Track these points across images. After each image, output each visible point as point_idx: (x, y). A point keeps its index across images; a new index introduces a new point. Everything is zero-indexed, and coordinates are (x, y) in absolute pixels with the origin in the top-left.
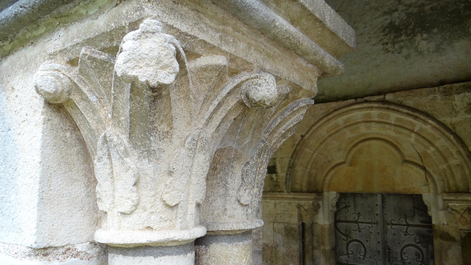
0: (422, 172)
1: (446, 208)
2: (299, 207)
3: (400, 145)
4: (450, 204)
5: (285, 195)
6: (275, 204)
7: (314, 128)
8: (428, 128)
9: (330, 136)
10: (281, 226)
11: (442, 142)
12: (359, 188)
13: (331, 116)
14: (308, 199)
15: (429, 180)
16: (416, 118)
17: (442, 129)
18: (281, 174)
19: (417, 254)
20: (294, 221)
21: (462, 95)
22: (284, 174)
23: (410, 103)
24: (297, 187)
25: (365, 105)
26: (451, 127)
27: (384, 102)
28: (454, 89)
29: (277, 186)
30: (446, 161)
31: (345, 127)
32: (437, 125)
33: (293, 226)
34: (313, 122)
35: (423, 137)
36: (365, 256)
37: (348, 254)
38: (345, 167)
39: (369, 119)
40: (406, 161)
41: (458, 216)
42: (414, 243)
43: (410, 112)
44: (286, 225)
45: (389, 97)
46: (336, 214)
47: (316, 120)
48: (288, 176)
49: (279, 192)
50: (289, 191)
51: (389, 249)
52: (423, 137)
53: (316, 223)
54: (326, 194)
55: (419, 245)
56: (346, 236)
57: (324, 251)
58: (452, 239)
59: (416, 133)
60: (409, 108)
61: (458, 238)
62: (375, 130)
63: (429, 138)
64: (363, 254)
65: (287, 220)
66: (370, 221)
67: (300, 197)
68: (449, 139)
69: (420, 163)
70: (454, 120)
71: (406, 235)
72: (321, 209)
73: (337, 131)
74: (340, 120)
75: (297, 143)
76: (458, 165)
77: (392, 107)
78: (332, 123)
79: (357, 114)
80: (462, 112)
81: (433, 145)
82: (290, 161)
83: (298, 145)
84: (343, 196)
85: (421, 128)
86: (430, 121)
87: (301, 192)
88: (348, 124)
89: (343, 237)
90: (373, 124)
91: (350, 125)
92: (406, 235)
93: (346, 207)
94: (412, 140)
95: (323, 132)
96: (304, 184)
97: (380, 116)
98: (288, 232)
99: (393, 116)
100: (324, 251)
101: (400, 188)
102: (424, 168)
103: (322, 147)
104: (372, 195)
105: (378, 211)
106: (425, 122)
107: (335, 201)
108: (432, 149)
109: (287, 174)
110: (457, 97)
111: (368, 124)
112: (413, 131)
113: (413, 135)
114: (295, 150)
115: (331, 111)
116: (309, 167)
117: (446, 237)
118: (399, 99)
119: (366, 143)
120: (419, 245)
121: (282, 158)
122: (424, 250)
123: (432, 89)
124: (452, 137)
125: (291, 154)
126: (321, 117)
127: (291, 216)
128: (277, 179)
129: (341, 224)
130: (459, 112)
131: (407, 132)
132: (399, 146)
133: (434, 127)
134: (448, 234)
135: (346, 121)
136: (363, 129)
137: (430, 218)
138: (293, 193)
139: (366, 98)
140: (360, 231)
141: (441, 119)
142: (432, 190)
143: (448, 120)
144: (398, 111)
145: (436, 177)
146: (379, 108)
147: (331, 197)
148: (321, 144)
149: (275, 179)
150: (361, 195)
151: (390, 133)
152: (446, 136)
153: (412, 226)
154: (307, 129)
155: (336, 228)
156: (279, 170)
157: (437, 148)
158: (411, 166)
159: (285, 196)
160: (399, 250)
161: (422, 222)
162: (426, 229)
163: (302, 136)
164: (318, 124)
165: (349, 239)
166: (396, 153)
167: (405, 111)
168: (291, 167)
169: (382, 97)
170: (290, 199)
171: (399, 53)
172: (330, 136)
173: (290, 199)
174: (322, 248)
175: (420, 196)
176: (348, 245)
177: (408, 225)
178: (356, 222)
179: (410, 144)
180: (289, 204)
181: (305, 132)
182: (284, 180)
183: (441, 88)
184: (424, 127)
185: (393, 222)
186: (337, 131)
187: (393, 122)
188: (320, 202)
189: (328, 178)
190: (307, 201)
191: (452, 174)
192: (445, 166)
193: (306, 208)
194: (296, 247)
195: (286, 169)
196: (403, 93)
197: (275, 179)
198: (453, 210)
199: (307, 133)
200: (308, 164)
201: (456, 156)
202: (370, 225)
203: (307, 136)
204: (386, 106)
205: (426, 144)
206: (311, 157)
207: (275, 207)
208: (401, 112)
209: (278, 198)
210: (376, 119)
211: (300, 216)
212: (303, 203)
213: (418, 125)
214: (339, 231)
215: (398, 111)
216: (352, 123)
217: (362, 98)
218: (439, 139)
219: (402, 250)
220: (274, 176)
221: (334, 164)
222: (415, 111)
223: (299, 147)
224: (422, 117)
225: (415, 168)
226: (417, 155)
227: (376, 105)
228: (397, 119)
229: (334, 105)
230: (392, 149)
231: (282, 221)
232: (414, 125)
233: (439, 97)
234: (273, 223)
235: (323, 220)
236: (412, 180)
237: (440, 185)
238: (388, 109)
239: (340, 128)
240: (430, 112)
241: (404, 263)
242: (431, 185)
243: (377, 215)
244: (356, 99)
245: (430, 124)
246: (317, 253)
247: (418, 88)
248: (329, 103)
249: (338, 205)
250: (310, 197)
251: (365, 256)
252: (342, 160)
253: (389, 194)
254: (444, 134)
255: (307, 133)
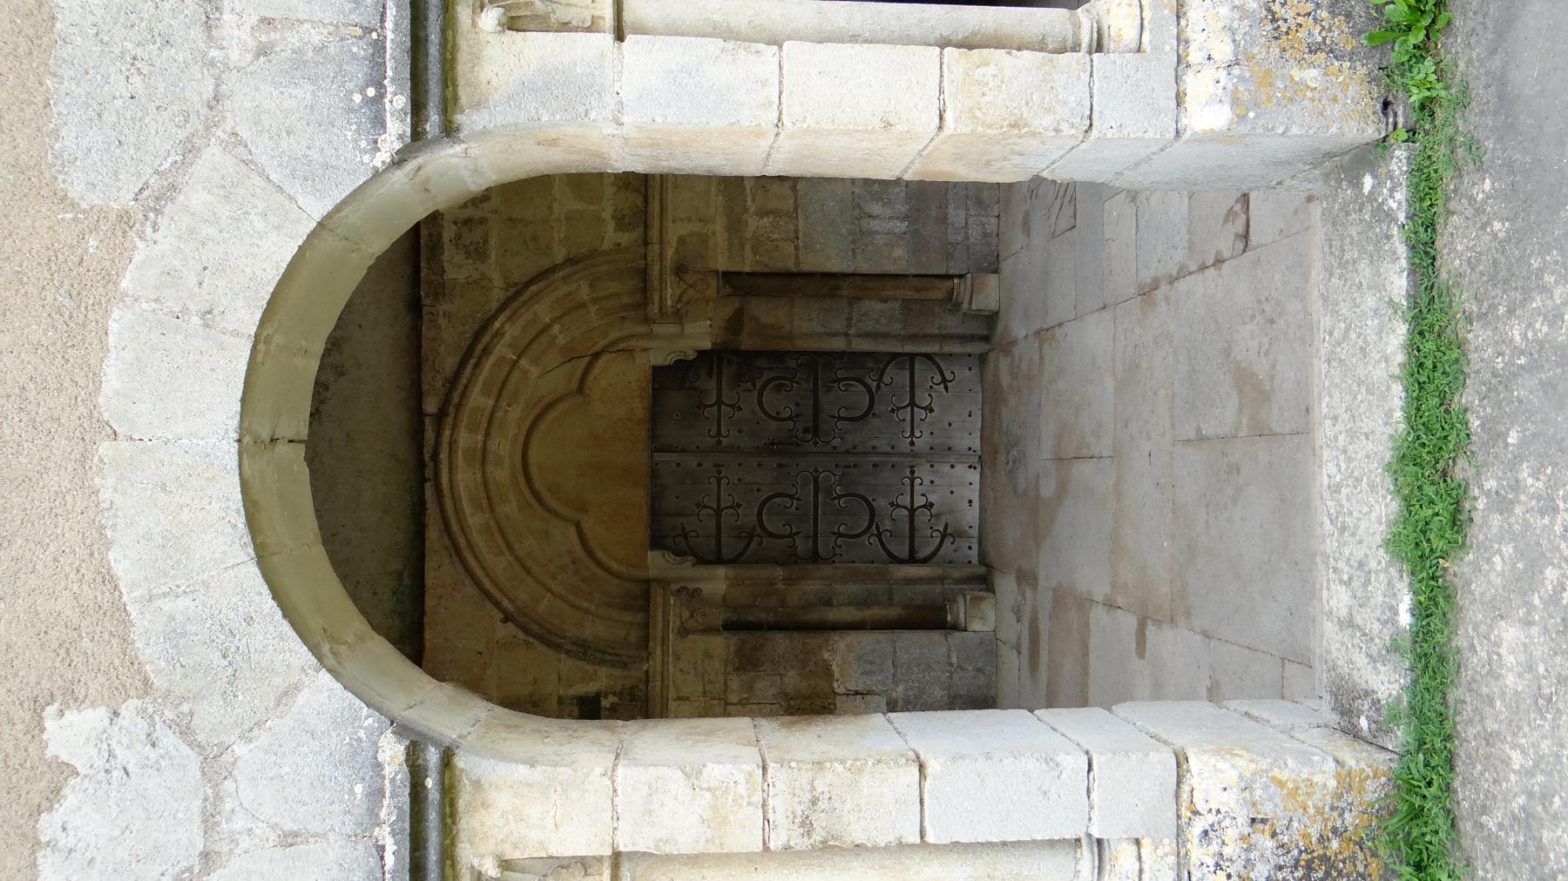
0: (605, 358)
1: (679, 317)
2: (684, 632)
3: (543, 397)
4: (669, 303)
5: (655, 664)
6: (679, 698)
7: (487, 584)
8: (511, 331)
9: (510, 547)
10: (735, 683)
11: (544, 310)
12: (640, 496)
13: (462, 541)
14: (666, 604)
15: (621, 346)
16: (486, 351)
17: (516, 304)
18: (601, 679)
19: (778, 388)
20: (720, 645)
21: (446, 265)
22: (603, 671)
23: (451, 363)
24: (635, 636)
25: (443, 456)
26: (512, 291)
27: (440, 417)
28: (433, 277)
29: (631, 695)
30: (583, 305)
31: (492, 510)
32: (507, 313)
33: (732, 648)
34: (471, 590)
35: (530, 343)
36: (792, 497)
37: (790, 535)
38: (588, 524)
39: (479, 453)
40: (580, 389)
41: (691, 292)
42: (756, 393)
43: (473, 361)
44: (730, 669)
45: (431, 405)
46: (702, 561)
47: (468, 581)
48: (608, 657)
49: (647, 681)
50: (644, 654)
51: (772, 444)
52: (530, 343)
53: (724, 598)
54: (653, 573)
55: (759, 383)
56: (751, 537)
57: (788, 580)
58: (739, 313)
59: (519, 357)
60: (462, 364)
61: (735, 303)
62: (504, 446)
63: (533, 331)
64: (788, 502)
65: (717, 664)
66: (713, 480)
67: (660, 625)
68: (536, 294)
69: (587, 359)
70: (498, 281)
71: (740, 409)
72: (691, 586)
73: (500, 529)
74: (474, 520)
75: (521, 635)
76: (591, 285)
77: (456, 400)
78: (479, 541)
79: (465, 479)
80: (482, 268)
81: (547, 327)
82: (568, 652)
83: (526, 631)
84: (656, 542)
85: (510, 346)
86: (497, 324)
87: (647, 626)
88: (485, 503)
89: (753, 545)
90: (492, 446)
91: (488, 498)
92: (740, 409)
93: (685, 535)
94: (534, 371)
95: (500, 564)
96: (628, 617)
97: (473, 429)
98: (747, 662)
99: (478, 399)
100: (788, 580)
101: (640, 408)
102: (596, 356)
103: (536, 570)
104: (654, 474)
105: (691, 462)
106: (499, 334)
107: (670, 557)
108: (556, 328)
109: (603, 662)
110: (450, 274)
111: (490, 458)
112: (515, 363)
113: (523, 362)
114: (540, 638)
115: (447, 541)
116: (586, 605)
117: (735, 323)
118: (439, 383)
119: (534, 471)
120: (759, 383)
121: (560, 678)
122: (767, 376)
123: (426, 318)
124: (533, 288)
125: (551, 653)
126: (460, 569)
127: (708, 655)
128: (614, 694)
129: (724, 550)
130: (482, 274)
131: (516, 374)
132: (547, 401)
133: (510, 319)
134: (729, 320)
135: (478, 507)
136: (500, 474)
137: (702, 354)
138: (651, 644)
139: (427, 456)
140: (739, 505)
141: (494, 305)
142: (643, 343)
143: (497, 295)
144: (466, 387)
145: (615, 334)
146: (454, 427)
147: (657, 563)
148: (528, 571)
149: (615, 699)
150: (655, 498)
151: (514, 415)
152: (531, 298)
153: (719, 395)
154: (489, 606)
155: (733, 561)
156: (591, 688)
157: (554, 320)
158: (591, 378)
159: (659, 669)
160: (773, 425)
161: (711, 376)
162: (725, 370)
163: (507, 618)
164: (479, 573)
165: (758, 531)
166: (560, 407)
167: (468, 370)
168: (582, 650)
169: (428, 421)
170: (664, 653)
171: (327, 388)
172: (510, 547)
173: (664, 653)
174: (780, 586)
175: (656, 370)
176: (771, 535)
177: (719, 403)
178: (718, 512)
179: (542, 377)
180: (677, 658)
181: (495, 610)
182: (617, 672)
183: (426, 301)
184: (507, 338)
185: (713, 433)
186: (500, 529)
187: (491, 402)
188: (674, 587)
189: (615, 566)
190: (670, 613)
191: (608, 297)
192: (593, 309)
193: (686, 614)
194: (781, 642)
195: (590, 668)
196: (427, 376)
197: (615, 699)
198: (680, 300)
199: (497, 604)
200: (578, 608)
201: (573, 287)
202: (724, 481)
203: (506, 603)
204: (452, 410)
205: (544, 339)
206: (560, 597)
207: (687, 699)
208: (469, 381)
209: (664, 687)
210: (480, 438)
211: (708, 630)
212: (674, 623)
213: (502, 350)
214: (742, 554)
215: (466, 387)
216: (483, 494)
217: (421, 465)
218: (535, 314)
219: (772, 417)
220: (605, 703)
221: (580, 552)
222: (473, 350)
223: (535, 627)
224: (486, 339)
225: (596, 372)
226: (568, 366)
227: (447, 432)
228: (486, 392)
229: (433, 534)
230: (552, 415)
231: (721, 678)
232: (502, 359)
233: (444, 307)
234: (727, 704)
235: (716, 582)
236: (621, 383)
237: (632, 328)
238: (459, 407)
239: (493, 524)
240: (476, 326)
241: (797, 416)
242: (634, 343)
243: (699, 465)
244: (424, 480)
245: (502, 325)
246: (793, 598)
247: (419, 346)
248: (427, 544)
249: (678, 553)
250: (660, 600)
251: (792, 497)
252: (572, 531)
253: (653, 436)
254: (525, 303)
255: (497, 604)
